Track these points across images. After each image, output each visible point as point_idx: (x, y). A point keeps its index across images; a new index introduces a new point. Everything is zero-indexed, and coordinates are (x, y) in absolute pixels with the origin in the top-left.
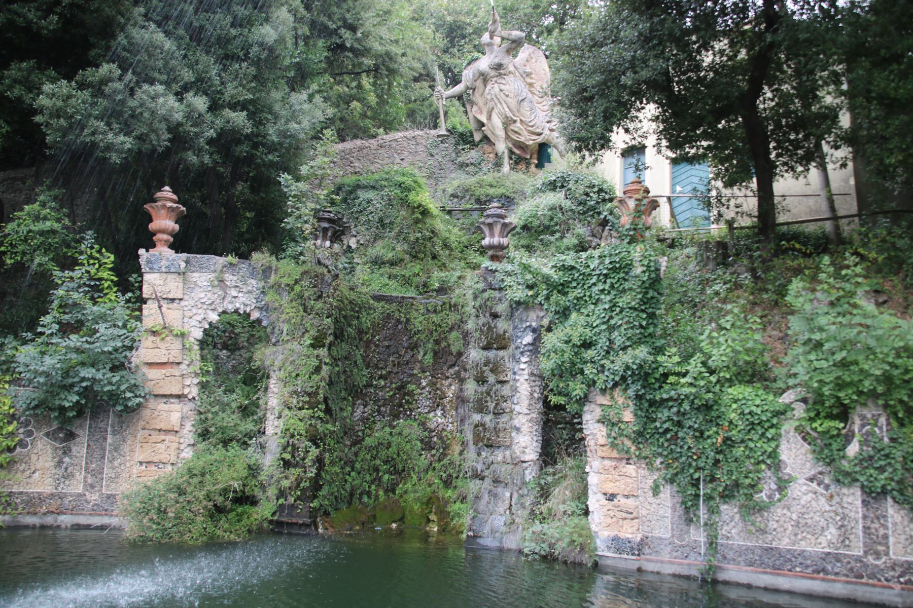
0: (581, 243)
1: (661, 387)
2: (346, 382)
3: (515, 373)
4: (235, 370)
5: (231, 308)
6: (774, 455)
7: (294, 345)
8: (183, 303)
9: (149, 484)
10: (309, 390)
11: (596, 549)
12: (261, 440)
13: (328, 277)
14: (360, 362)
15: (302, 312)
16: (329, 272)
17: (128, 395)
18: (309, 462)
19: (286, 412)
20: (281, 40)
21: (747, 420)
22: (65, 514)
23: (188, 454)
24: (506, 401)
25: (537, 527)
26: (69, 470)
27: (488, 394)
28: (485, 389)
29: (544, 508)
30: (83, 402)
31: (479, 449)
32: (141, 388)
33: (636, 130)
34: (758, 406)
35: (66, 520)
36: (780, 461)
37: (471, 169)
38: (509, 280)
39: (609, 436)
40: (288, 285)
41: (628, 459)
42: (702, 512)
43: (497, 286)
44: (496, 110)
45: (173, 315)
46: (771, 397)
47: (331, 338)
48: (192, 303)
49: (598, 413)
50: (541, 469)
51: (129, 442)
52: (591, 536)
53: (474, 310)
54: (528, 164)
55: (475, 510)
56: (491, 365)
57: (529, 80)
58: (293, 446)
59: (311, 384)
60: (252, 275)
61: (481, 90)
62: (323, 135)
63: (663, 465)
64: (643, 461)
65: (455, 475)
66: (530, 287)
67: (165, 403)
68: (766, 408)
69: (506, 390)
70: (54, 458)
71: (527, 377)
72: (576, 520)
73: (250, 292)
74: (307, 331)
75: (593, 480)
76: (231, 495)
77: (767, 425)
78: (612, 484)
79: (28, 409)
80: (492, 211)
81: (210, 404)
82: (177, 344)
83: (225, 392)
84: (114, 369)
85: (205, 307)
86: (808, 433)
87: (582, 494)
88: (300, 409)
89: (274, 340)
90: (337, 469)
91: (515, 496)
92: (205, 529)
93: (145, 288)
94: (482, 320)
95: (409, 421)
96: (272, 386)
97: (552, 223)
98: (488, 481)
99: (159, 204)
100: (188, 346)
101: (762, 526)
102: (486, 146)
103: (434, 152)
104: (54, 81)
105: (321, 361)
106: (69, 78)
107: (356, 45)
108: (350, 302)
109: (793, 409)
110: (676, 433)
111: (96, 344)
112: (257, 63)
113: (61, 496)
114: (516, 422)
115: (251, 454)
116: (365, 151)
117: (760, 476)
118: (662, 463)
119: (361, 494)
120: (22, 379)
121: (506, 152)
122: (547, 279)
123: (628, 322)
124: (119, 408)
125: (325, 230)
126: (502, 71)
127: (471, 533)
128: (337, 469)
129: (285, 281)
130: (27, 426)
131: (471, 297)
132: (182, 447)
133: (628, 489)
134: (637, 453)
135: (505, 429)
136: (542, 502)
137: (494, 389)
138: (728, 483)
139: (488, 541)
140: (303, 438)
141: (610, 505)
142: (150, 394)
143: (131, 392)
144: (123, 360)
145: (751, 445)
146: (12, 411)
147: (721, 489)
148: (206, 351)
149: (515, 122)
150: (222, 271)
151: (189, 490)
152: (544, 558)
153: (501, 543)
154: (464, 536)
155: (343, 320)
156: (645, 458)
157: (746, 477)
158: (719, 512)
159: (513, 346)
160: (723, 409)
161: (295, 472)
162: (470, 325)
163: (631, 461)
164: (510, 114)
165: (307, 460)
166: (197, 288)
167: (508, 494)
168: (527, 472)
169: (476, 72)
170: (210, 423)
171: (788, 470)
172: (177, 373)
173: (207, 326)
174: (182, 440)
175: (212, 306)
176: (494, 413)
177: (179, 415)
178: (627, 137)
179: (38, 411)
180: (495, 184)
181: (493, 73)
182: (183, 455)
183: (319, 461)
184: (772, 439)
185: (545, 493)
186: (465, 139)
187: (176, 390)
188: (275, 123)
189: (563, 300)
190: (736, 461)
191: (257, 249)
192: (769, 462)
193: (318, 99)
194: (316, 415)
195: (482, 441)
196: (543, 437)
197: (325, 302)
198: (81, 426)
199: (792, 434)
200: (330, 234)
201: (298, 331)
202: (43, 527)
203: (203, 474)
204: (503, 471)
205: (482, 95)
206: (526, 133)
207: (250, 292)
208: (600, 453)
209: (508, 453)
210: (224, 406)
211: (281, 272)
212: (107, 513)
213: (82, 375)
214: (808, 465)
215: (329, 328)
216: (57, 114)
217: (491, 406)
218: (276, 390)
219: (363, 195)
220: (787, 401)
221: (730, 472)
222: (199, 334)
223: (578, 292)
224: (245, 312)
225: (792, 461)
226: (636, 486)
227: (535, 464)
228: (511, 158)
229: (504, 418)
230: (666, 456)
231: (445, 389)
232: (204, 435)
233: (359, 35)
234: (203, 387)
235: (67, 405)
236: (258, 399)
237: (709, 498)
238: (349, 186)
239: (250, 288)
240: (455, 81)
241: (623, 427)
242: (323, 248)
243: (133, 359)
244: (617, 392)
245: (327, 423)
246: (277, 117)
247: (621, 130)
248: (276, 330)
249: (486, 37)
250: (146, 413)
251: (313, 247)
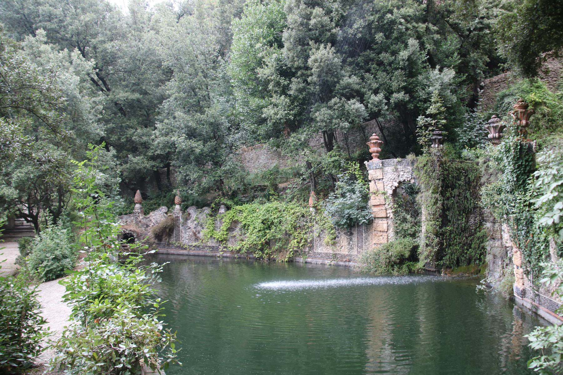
8: (384, 180)
45: (380, 185)
48: (387, 180)
60: (408, 165)
73: (408, 172)
113: (351, 256)
191: (408, 154)
198: (354, 230)
202: (346, 266)
207: (408, 172)
219: (506, 100)
250: (374, 225)
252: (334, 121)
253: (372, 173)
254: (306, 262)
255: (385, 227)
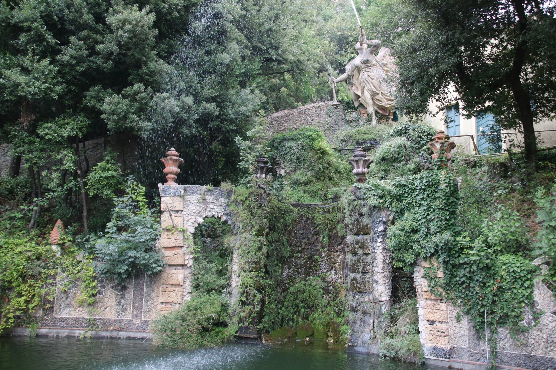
0: (417, 166)
1: (459, 256)
2: (277, 255)
3: (374, 249)
4: (215, 249)
5: (210, 214)
6: (530, 297)
7: (246, 235)
8: (183, 213)
9: (166, 315)
10: (255, 260)
11: (423, 354)
12: (229, 289)
13: (264, 195)
14: (285, 243)
15: (250, 216)
16: (265, 192)
17: (154, 265)
18: (256, 302)
19: (243, 273)
20: (234, 60)
21: (512, 276)
22: (122, 331)
23: (188, 298)
24: (369, 265)
25: (388, 340)
26: (124, 307)
27: (359, 261)
28: (356, 258)
29: (393, 329)
30: (130, 269)
31: (354, 294)
32: (161, 261)
33: (444, 99)
34: (518, 267)
35: (123, 334)
36: (534, 301)
37: (353, 124)
38: (368, 193)
39: (429, 286)
40: (242, 201)
41: (441, 300)
42: (487, 333)
43: (362, 197)
44: (366, 88)
46: (527, 262)
47: (267, 230)
48: (188, 212)
49: (422, 272)
50: (392, 305)
51: (156, 291)
52: (420, 346)
53: (348, 212)
54: (388, 119)
55: (353, 330)
56: (360, 244)
57: (385, 68)
58: (247, 293)
59: (256, 257)
60: (221, 196)
61: (357, 76)
62: (259, 113)
63: (462, 304)
64: (450, 301)
65: (343, 309)
66: (381, 197)
67: (175, 269)
68: (523, 268)
69: (369, 259)
70: (116, 300)
71: (381, 251)
72: (411, 336)
73: (220, 205)
74: (253, 227)
75: (421, 312)
76: (211, 322)
77: (524, 279)
78: (432, 315)
79: (102, 274)
80: (358, 153)
81: (200, 269)
82: (181, 236)
83: (208, 262)
84: (146, 251)
85: (195, 214)
86: (551, 284)
87: (415, 322)
88: (250, 271)
89: (235, 232)
90: (273, 306)
91: (376, 322)
92: (197, 340)
93: (162, 205)
94: (354, 218)
95: (315, 277)
96: (234, 259)
97: (400, 156)
98: (360, 313)
99: (168, 158)
100: (186, 237)
101: (524, 342)
102: (361, 110)
103: (331, 114)
104: (110, 95)
105: (262, 244)
106: (118, 92)
107: (279, 58)
108: (279, 209)
109: (541, 269)
110: (469, 284)
111: (137, 238)
112: (222, 74)
113: (120, 321)
114: (375, 278)
115: (224, 298)
116: (290, 117)
117: (522, 310)
118: (461, 302)
119: (288, 321)
120: (99, 257)
121: (374, 112)
122: (390, 193)
123: (438, 217)
124: (149, 273)
125: (262, 168)
126: (369, 65)
127: (350, 344)
128: (273, 306)
129: (240, 198)
130: (102, 282)
131: (347, 204)
132: (185, 294)
133: (442, 318)
134: (446, 296)
135: (369, 282)
136: (392, 325)
137: (362, 258)
138: (502, 315)
139: (360, 349)
140: (252, 288)
141: (431, 327)
142: (166, 264)
143: (156, 263)
144: (151, 246)
145: (515, 291)
146: (94, 274)
147: (497, 318)
148: (197, 239)
149: (378, 94)
150: (204, 194)
151: (188, 319)
152: (394, 358)
153: (368, 350)
154: (347, 345)
155: (274, 219)
156: (452, 299)
157: (513, 311)
158: (497, 333)
159: (372, 233)
160: (497, 269)
161: (248, 308)
162: (347, 221)
163: (443, 301)
164: (374, 90)
165: (255, 301)
166: (191, 204)
167: (372, 321)
168: (383, 307)
169: (353, 66)
170: (200, 280)
171: (539, 307)
172: (181, 253)
173: (197, 226)
174: (184, 290)
175: (199, 214)
176: (362, 273)
177: (182, 276)
178: (438, 104)
179: (107, 275)
180: (367, 132)
181: (363, 66)
182: (185, 298)
183: (262, 301)
184: (528, 287)
185: (394, 320)
186: (349, 106)
187: (180, 262)
188: (233, 108)
189: (400, 205)
190: (506, 301)
191: (224, 180)
192: (526, 302)
193: (257, 92)
194: (260, 275)
195: (356, 289)
196: (392, 286)
197: (263, 210)
199: (541, 284)
200: (265, 170)
201: (248, 227)
202: (111, 338)
203: (196, 310)
204: (369, 307)
205: (358, 79)
206: (385, 100)
207: (220, 205)
208: (424, 296)
209: (371, 296)
210: (207, 270)
211: (238, 193)
212: (144, 331)
213: (129, 255)
214: (552, 304)
215: (266, 224)
216: (113, 113)
217: (361, 268)
218: (237, 261)
219: (287, 144)
220: (537, 264)
221: (502, 308)
222: (192, 230)
223: (409, 200)
224: (218, 217)
225: (541, 301)
226: (446, 316)
227: (388, 303)
228: (376, 116)
229: (368, 275)
230: (464, 298)
231: (336, 258)
232: (197, 287)
233: (280, 52)
234: (196, 260)
235: (122, 271)
236: (227, 266)
237: (491, 324)
238: (279, 139)
239: (220, 203)
240: (342, 71)
241: (437, 280)
242: (262, 178)
243: (156, 245)
244: (434, 259)
245: (267, 279)
246: (234, 104)
247: (434, 100)
248: (236, 226)
249: (358, 45)
250: (164, 275)
251: (255, 178)
252: (131, 116)
253: (166, 202)
254: (37, 336)
255: (180, 278)
